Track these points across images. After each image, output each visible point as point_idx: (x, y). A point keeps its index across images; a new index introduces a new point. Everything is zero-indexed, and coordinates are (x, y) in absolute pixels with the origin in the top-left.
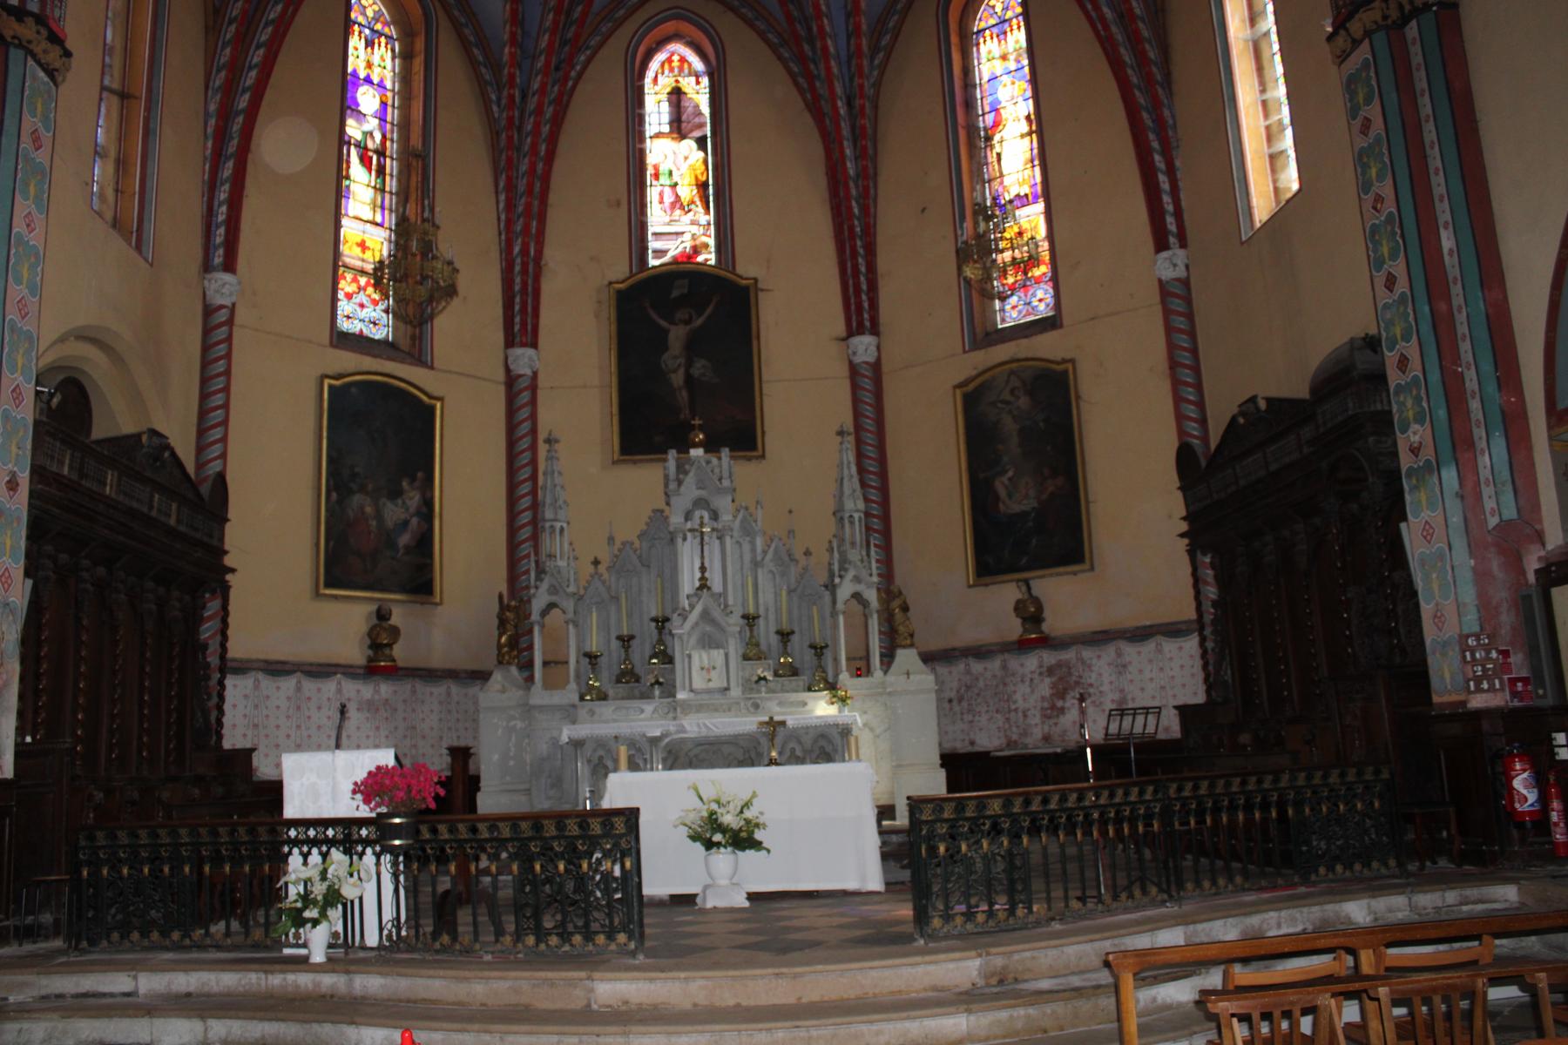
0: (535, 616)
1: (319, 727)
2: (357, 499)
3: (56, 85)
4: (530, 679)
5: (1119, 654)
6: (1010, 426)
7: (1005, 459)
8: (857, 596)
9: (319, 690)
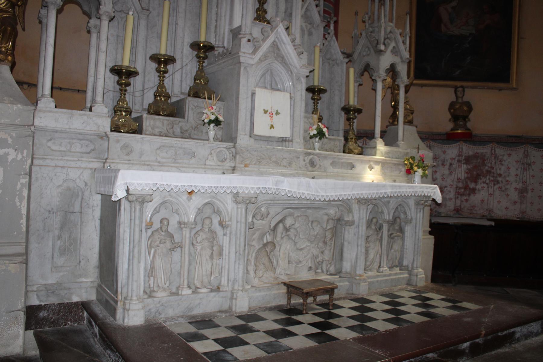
5: (526, 155)
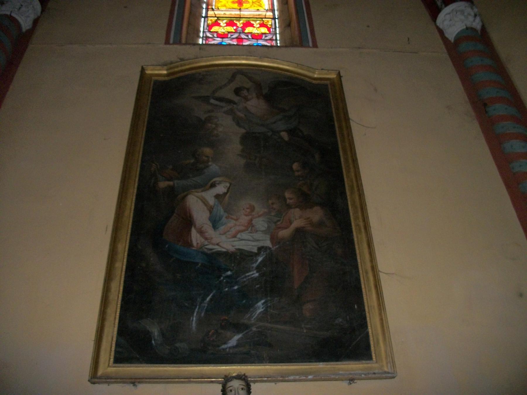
7: (214, 167)
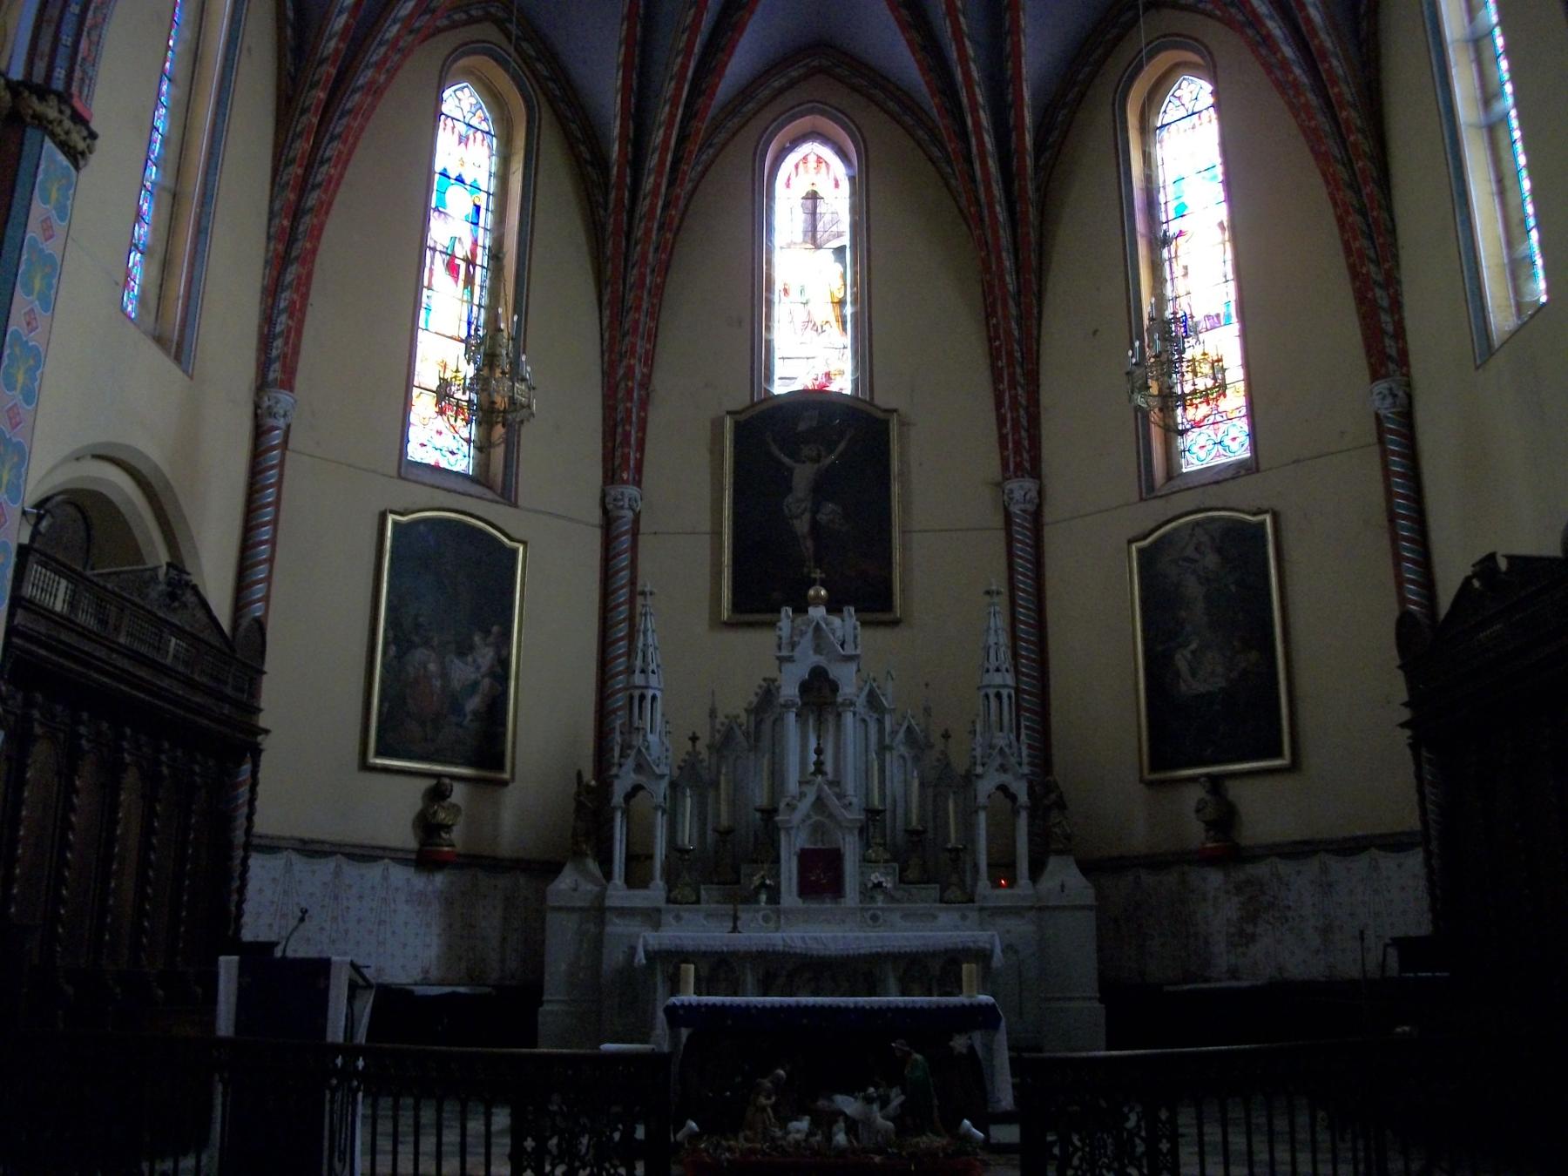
0: (618, 799)
1: (359, 921)
2: (419, 654)
3: (77, 168)
4: (608, 875)
6: (1193, 588)
7: (1189, 628)
8: (1003, 788)
9: (362, 876)
